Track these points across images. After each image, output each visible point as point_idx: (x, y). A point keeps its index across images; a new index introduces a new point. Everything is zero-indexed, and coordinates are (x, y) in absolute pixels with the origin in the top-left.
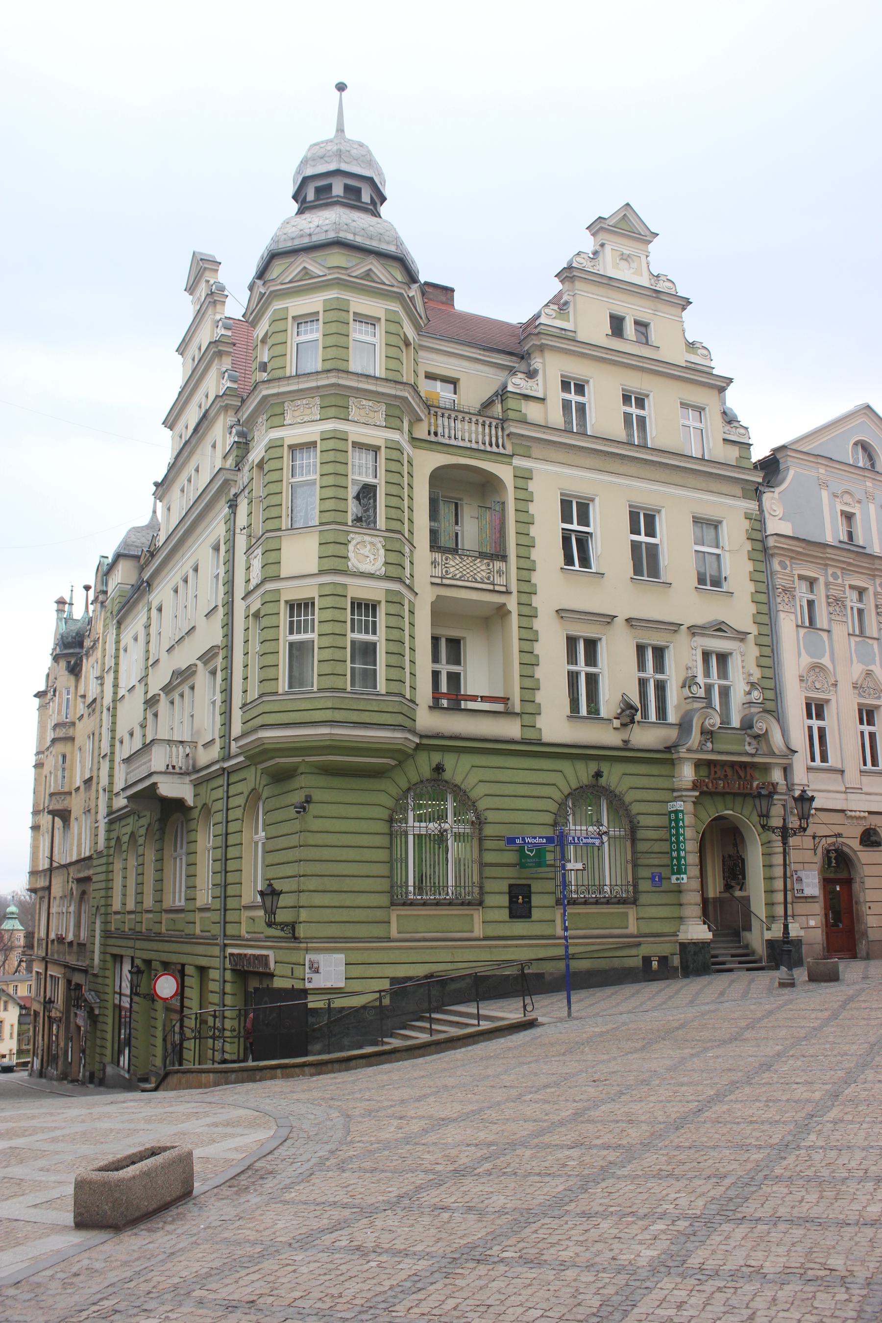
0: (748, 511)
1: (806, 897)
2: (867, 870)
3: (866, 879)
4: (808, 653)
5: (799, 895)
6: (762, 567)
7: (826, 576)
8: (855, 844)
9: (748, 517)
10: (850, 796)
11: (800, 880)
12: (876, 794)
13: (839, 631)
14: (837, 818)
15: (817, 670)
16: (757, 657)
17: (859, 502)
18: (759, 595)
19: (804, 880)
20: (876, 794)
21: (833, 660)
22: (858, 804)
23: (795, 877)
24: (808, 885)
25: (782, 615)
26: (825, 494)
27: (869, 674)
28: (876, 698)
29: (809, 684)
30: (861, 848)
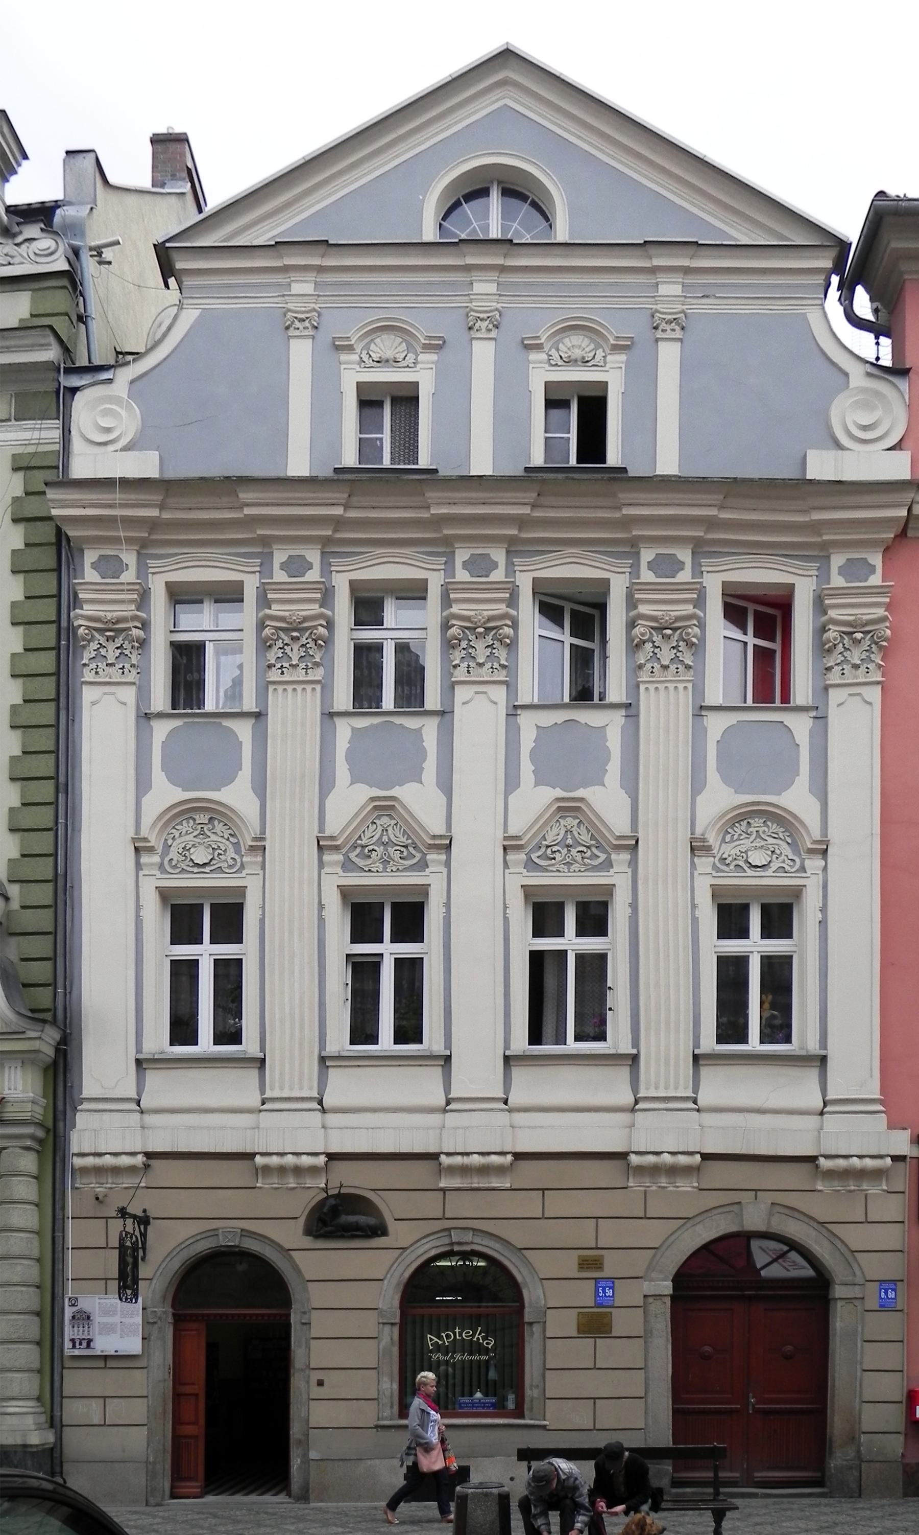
0: (19, 450)
1: (106, 1358)
2: (318, 1295)
3: (315, 1316)
4: (174, 779)
5: (77, 1352)
6: (48, 584)
7: (265, 568)
8: (291, 1235)
9: (21, 465)
10: (266, 1119)
11: (83, 1318)
12: (374, 1110)
13: (294, 713)
14: (234, 1173)
15: (202, 818)
16: (12, 810)
17: (437, 346)
18: (33, 657)
19: (97, 1319)
20: (374, 1110)
21: (260, 787)
22: (296, 1136)
23: (69, 1312)
24: (108, 1329)
25: (88, 695)
26: (301, 353)
27: (384, 808)
28: (411, 868)
29: (173, 854)
30: (308, 1242)
